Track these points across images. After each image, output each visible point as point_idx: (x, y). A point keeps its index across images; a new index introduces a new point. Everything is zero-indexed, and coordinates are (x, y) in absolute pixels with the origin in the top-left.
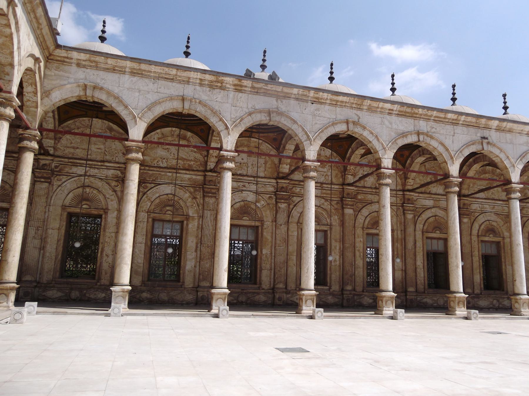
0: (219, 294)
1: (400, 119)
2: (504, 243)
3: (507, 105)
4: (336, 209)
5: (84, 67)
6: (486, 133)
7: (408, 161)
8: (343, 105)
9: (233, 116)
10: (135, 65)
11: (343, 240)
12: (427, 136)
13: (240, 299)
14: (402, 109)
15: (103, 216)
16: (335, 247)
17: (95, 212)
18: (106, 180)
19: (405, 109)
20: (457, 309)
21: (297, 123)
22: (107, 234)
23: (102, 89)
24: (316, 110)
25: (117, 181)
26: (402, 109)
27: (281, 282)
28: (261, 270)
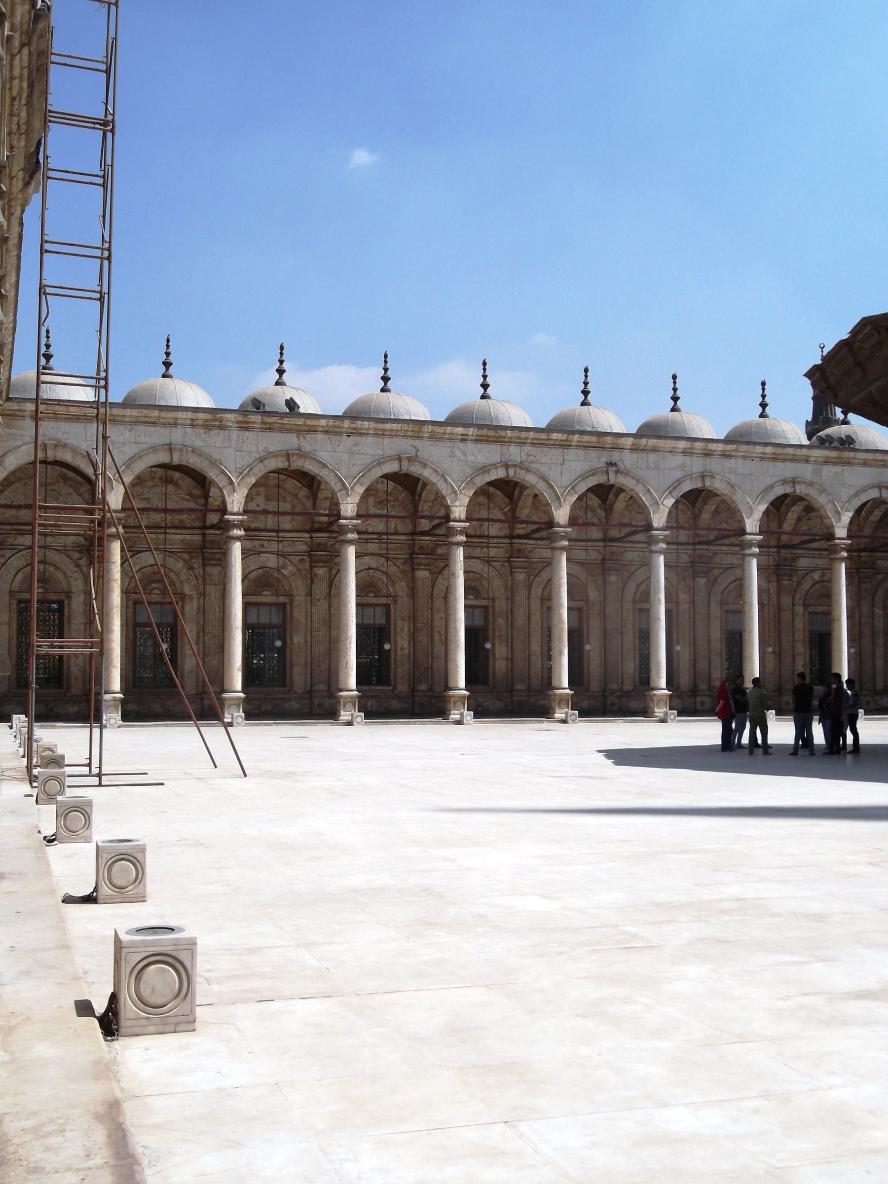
1: (479, 446)
2: (678, 611)
4: (403, 572)
6: (615, 456)
7: (516, 492)
8: (392, 434)
9: (238, 466)
11: (413, 618)
12: (521, 468)
13: (263, 708)
14: (481, 432)
15: (66, 602)
16: (402, 629)
19: (485, 432)
20: (557, 710)
21: (327, 467)
23: (65, 446)
24: (354, 445)
25: (80, 551)
26: (481, 432)
27: (321, 682)
28: (292, 667)
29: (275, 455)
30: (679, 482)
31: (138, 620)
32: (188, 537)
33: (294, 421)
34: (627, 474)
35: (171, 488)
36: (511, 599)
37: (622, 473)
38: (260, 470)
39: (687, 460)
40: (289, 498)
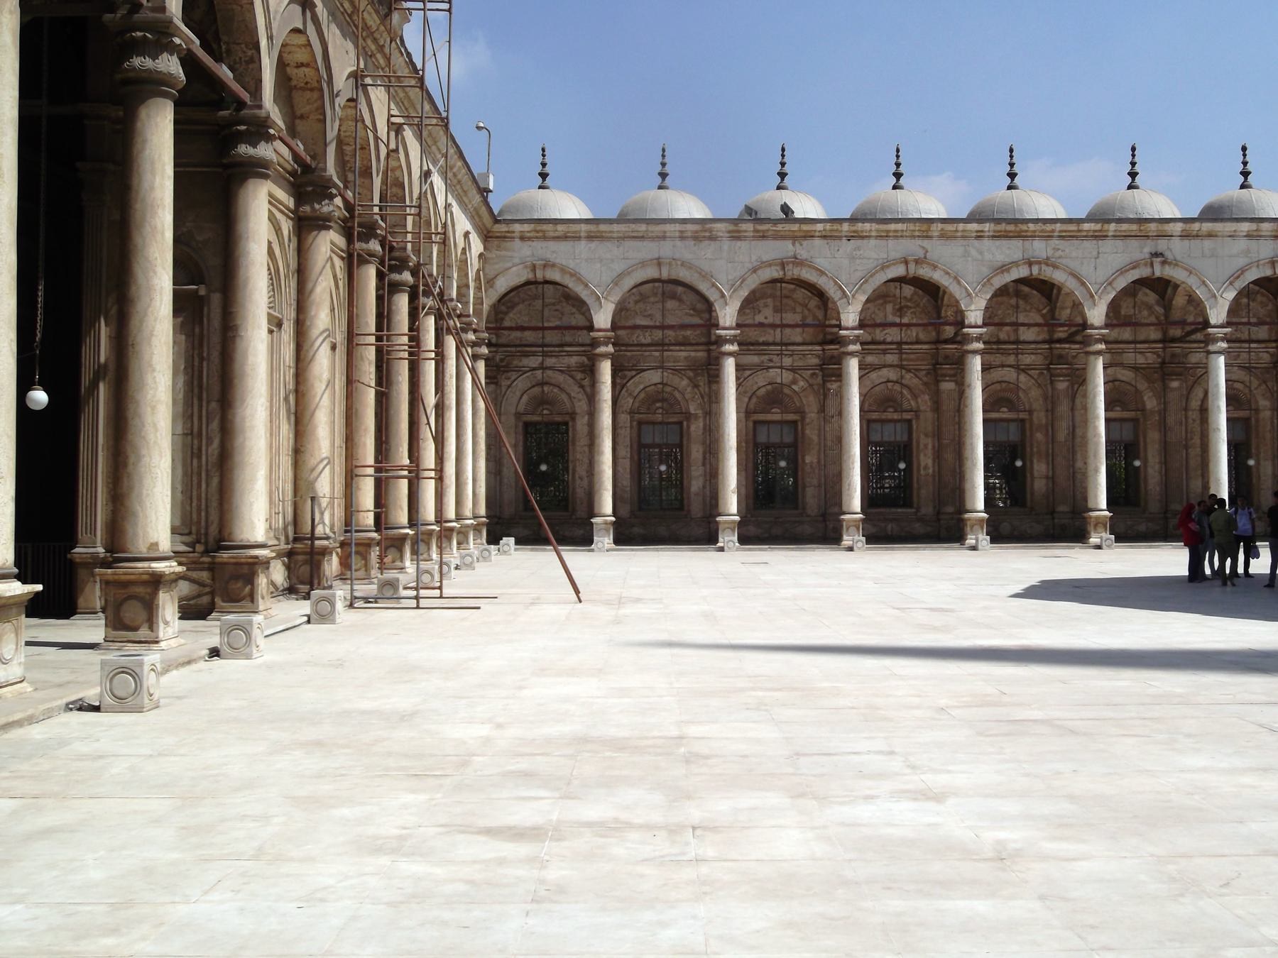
0: (726, 522)
1: (998, 243)
2: (1257, 420)
3: (1249, 167)
4: (925, 384)
5: (530, 239)
6: (1162, 245)
8: (898, 236)
10: (592, 227)
11: (938, 434)
14: (999, 227)
16: (926, 446)
17: (558, 419)
18: (568, 371)
19: (1003, 227)
20: (1093, 534)
22: (578, 448)
23: (553, 265)
25: (583, 372)
26: (999, 227)
28: (804, 488)
29: (770, 264)
30: (1243, 271)
31: (643, 441)
32: (693, 354)
33: (788, 227)
34: (1176, 264)
35: (671, 304)
36: (1051, 410)
37: (1170, 264)
38: (753, 282)
39: (1253, 244)
40: (799, 309)
